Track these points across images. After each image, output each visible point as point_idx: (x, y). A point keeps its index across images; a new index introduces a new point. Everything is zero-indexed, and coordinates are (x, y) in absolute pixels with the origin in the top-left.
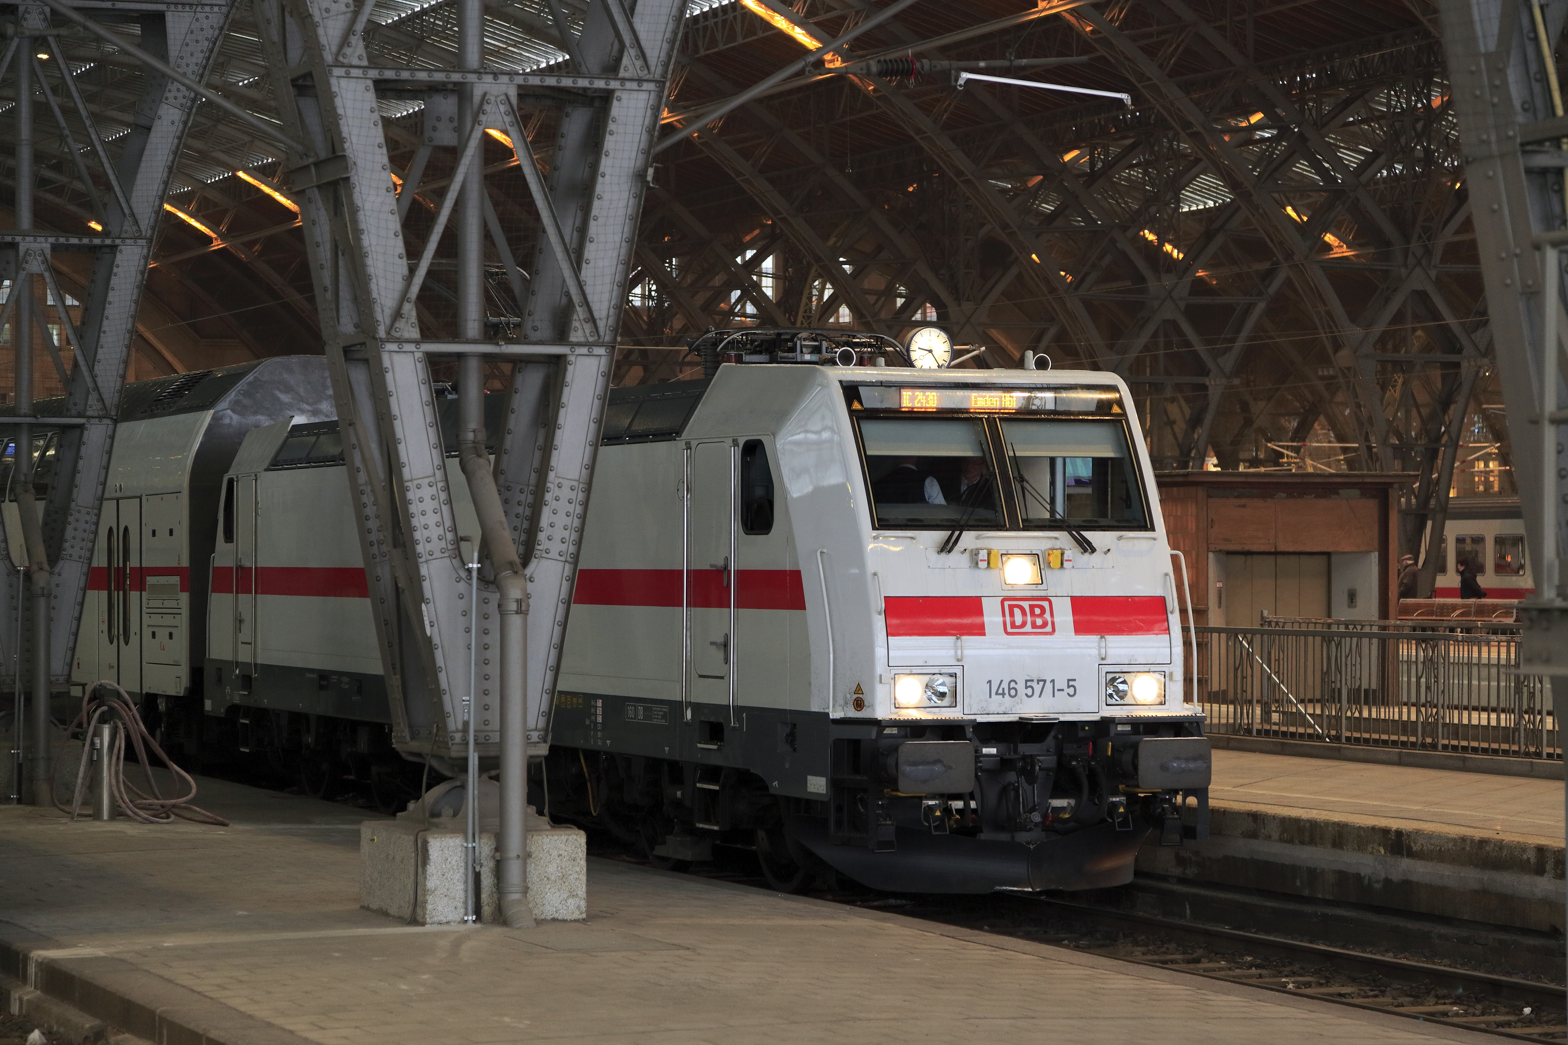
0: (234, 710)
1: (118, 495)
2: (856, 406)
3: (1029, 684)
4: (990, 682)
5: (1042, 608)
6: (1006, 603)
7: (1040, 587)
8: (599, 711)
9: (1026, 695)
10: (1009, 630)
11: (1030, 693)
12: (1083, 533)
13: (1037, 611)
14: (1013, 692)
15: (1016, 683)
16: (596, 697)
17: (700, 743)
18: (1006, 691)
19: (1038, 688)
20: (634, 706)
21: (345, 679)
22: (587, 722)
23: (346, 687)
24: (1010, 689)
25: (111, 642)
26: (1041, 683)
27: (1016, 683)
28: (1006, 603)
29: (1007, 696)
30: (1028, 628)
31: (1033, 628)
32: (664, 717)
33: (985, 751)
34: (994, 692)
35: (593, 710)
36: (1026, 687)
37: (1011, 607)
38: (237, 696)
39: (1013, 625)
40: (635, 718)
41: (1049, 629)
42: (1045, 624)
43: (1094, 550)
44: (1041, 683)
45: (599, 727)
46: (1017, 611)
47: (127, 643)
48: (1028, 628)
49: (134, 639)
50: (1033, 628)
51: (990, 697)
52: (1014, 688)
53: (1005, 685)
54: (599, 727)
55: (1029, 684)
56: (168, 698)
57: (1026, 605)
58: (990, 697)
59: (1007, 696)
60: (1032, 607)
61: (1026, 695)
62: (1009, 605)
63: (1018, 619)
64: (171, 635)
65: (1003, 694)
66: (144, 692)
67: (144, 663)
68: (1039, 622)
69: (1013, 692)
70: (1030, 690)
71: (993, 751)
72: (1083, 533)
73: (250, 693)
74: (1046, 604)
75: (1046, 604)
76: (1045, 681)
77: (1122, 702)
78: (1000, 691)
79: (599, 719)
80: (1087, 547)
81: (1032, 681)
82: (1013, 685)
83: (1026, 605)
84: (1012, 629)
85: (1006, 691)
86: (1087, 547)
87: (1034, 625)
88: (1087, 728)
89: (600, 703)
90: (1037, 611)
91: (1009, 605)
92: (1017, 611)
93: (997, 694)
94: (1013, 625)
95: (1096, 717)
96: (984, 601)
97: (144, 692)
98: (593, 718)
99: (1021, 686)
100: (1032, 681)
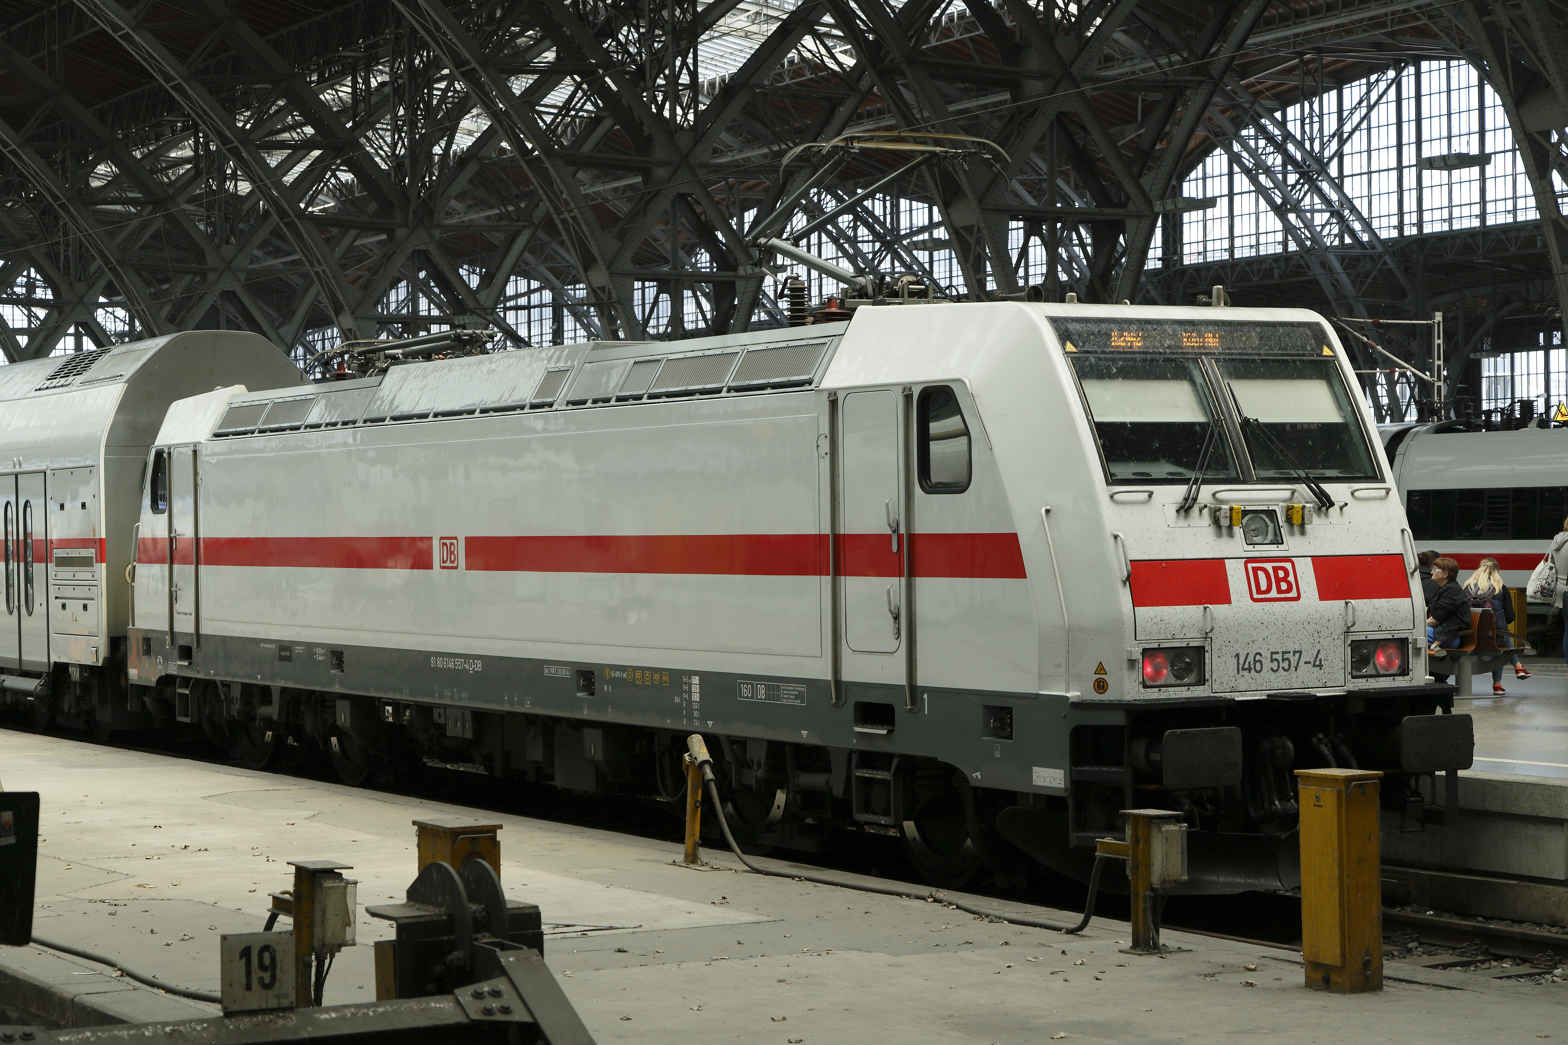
0: (167, 681)
1: (17, 469)
3: (1274, 656)
4: (1237, 656)
8: (696, 689)
9: (1272, 669)
11: (1275, 668)
13: (1281, 574)
16: (691, 673)
17: (857, 725)
18: (1252, 667)
20: (752, 685)
21: (321, 651)
22: (677, 700)
23: (321, 658)
25: (11, 613)
26: (1297, 655)
28: (1250, 566)
29: (1253, 671)
30: (1274, 594)
31: (1278, 593)
32: (797, 697)
35: (685, 687)
36: (1272, 661)
37: (1255, 570)
38: (176, 667)
39: (1259, 591)
40: (752, 697)
41: (1293, 594)
42: (1289, 589)
44: (1297, 655)
45: (696, 706)
46: (1261, 574)
47: (30, 614)
48: (1274, 594)
49: (39, 610)
50: (1278, 593)
53: (1251, 658)
54: (696, 706)
55: (1274, 656)
56: (82, 667)
57: (1269, 566)
59: (1253, 671)
60: (1275, 569)
62: (1253, 568)
64: (85, 607)
65: (1249, 669)
66: (52, 661)
67: (52, 635)
70: (1275, 662)
73: (190, 664)
74: (1288, 565)
75: (1288, 565)
78: (1246, 666)
79: (696, 697)
81: (1289, 652)
85: (1252, 667)
86: (1325, 502)
87: (1279, 591)
89: (696, 680)
90: (1281, 574)
91: (1253, 568)
92: (1261, 574)
93: (1243, 669)
94: (1259, 591)
97: (52, 661)
98: (686, 696)
100: (1278, 653)
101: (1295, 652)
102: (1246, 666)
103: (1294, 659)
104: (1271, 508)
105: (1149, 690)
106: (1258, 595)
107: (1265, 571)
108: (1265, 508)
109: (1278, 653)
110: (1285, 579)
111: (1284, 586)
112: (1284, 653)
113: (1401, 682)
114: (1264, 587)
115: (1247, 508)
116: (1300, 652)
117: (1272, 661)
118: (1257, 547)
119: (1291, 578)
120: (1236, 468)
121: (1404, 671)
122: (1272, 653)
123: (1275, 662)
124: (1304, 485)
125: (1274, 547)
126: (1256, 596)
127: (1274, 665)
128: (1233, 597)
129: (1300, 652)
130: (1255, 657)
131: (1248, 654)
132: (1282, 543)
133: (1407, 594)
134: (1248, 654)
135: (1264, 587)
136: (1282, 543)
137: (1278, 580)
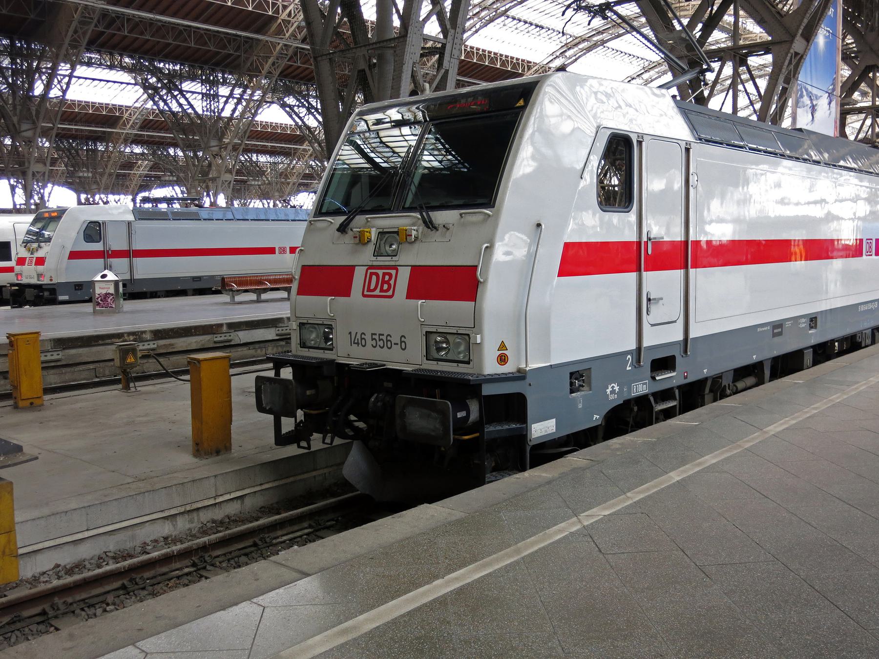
3: (374, 337)
4: (350, 333)
5: (390, 275)
9: (372, 345)
11: (374, 345)
13: (387, 278)
18: (360, 342)
24: (362, 339)
28: (370, 271)
29: (360, 345)
30: (377, 292)
36: (373, 339)
37: (372, 274)
41: (390, 293)
52: (364, 339)
53: (358, 336)
55: (374, 337)
59: (360, 345)
60: (384, 274)
61: (372, 345)
65: (358, 344)
75: (393, 272)
78: (356, 341)
85: (360, 342)
86: (429, 225)
87: (382, 290)
90: (387, 278)
93: (354, 343)
99: (368, 337)
102: (356, 341)
107: (377, 275)
111: (386, 287)
112: (380, 335)
114: (372, 287)
115: (385, 230)
117: (373, 339)
119: (392, 282)
122: (372, 334)
123: (374, 341)
125: (389, 258)
127: (374, 343)
135: (372, 287)
137: (384, 282)
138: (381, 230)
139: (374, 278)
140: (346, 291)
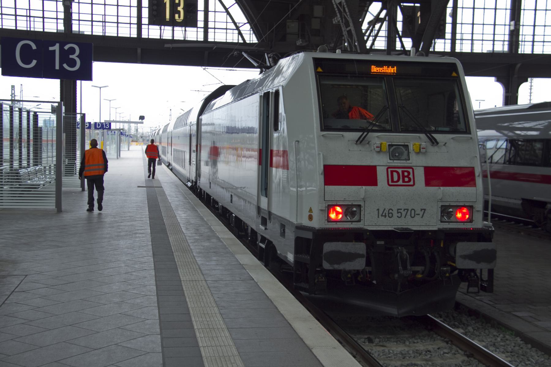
2: (320, 70)
3: (399, 211)
4: (378, 210)
5: (409, 173)
6: (389, 170)
7: (408, 162)
9: (398, 217)
10: (390, 183)
11: (399, 216)
12: (433, 135)
13: (406, 174)
14: (390, 215)
15: (392, 210)
18: (387, 215)
19: (404, 213)
24: (389, 214)
27: (392, 210)
28: (389, 170)
29: (387, 217)
30: (401, 182)
33: (378, 243)
34: (380, 215)
36: (398, 213)
37: (392, 172)
39: (393, 181)
41: (411, 183)
43: (437, 143)
48: (401, 182)
51: (378, 217)
52: (391, 213)
55: (399, 211)
57: (400, 171)
58: (378, 217)
59: (387, 217)
60: (403, 172)
61: (398, 217)
63: (395, 179)
65: (385, 216)
68: (406, 179)
69: (390, 215)
70: (400, 214)
71: (383, 243)
72: (433, 135)
74: (410, 170)
75: (410, 170)
76: (408, 210)
77: (449, 220)
78: (384, 214)
80: (434, 142)
82: (391, 211)
83: (400, 171)
84: (391, 183)
85: (387, 215)
86: (434, 142)
87: (404, 181)
88: (430, 234)
90: (406, 174)
93: (382, 216)
94: (393, 181)
95: (435, 228)
96: (378, 168)
100: (401, 209)
101: (404, 210)
103: (404, 213)
104: (406, 144)
105: (330, 223)
106: (391, 183)
108: (403, 144)
109: (401, 209)
110: (408, 176)
111: (406, 179)
113: (469, 226)
115: (393, 143)
116: (425, 210)
118: (395, 161)
119: (411, 176)
120: (391, 126)
121: (471, 220)
122: (398, 209)
123: (400, 214)
124: (424, 135)
125: (405, 161)
126: (390, 183)
127: (399, 215)
128: (379, 184)
129: (425, 210)
130: (389, 211)
131: (385, 209)
132: (409, 160)
133: (475, 185)
134: (385, 209)
136: (409, 160)
137: (404, 177)
138: (390, 143)
139: (395, 175)
140: (373, 182)
